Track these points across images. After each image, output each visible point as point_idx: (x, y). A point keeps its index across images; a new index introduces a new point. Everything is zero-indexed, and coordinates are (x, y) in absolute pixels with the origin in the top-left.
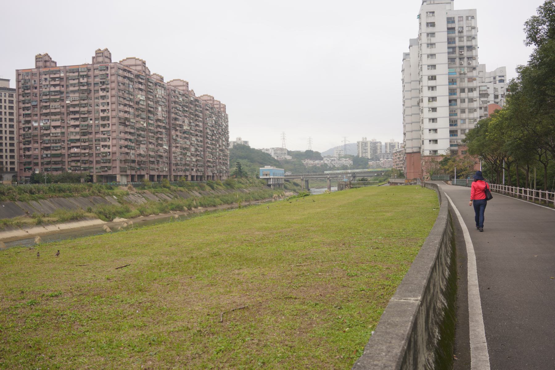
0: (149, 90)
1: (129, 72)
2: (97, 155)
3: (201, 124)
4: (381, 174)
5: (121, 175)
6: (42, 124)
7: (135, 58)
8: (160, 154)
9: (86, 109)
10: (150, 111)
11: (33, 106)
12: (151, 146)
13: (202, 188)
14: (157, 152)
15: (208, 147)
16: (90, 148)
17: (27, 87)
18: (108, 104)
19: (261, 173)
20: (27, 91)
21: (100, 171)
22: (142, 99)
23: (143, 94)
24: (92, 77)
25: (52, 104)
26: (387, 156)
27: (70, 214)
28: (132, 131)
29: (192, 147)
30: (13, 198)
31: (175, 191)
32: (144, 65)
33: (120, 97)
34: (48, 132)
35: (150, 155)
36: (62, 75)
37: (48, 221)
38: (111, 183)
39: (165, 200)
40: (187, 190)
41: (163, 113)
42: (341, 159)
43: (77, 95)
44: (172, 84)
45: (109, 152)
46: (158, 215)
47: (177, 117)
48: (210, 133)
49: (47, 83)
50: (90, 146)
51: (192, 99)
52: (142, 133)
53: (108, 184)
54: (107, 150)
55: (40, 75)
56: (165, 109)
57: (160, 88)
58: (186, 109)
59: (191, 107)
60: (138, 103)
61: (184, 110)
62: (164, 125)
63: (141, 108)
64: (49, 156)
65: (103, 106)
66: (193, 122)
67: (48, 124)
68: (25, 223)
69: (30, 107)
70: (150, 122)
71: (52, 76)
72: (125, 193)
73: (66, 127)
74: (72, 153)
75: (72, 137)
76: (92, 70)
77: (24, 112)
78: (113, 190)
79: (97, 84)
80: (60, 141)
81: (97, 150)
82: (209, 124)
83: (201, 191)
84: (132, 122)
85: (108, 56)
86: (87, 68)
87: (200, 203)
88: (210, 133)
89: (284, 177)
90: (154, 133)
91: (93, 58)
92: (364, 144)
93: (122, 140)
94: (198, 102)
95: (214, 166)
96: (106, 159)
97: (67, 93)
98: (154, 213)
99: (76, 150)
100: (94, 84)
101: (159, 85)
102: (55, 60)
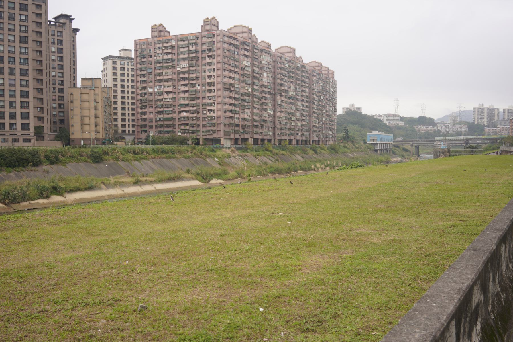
0: (254, 56)
1: (235, 39)
2: (204, 119)
3: (307, 90)
4: (497, 141)
5: (225, 138)
6: (156, 90)
7: (241, 26)
8: (264, 118)
9: (194, 75)
11: (148, 73)
12: (255, 111)
13: (305, 152)
14: (261, 117)
15: (314, 112)
16: (198, 113)
17: (143, 55)
19: (368, 138)
20: (143, 60)
21: (206, 134)
22: (247, 65)
25: (166, 71)
26: (505, 123)
27: (167, 175)
28: (237, 96)
29: (297, 112)
31: (277, 154)
32: (250, 32)
33: (225, 63)
34: (161, 97)
35: (254, 119)
36: (174, 43)
37: (146, 180)
38: (215, 146)
39: (266, 163)
40: (289, 154)
41: (269, 79)
42: (455, 125)
43: (187, 62)
44: (280, 51)
45: (214, 116)
47: (283, 83)
49: (161, 51)
50: (198, 110)
51: (299, 65)
52: (247, 98)
53: (212, 146)
54: (212, 114)
55: (155, 44)
56: (270, 75)
57: (266, 54)
58: (292, 75)
59: (297, 73)
60: (243, 69)
61: (291, 76)
62: (269, 90)
63: (246, 74)
64: (162, 119)
65: (210, 72)
66: (299, 88)
67: (162, 90)
68: (123, 182)
69: (146, 74)
70: (255, 87)
71: (165, 45)
72: (226, 155)
73: (177, 93)
75: (182, 102)
76: (200, 38)
77: (141, 79)
78: (215, 152)
79: (205, 51)
80: (171, 106)
81: (204, 114)
82: (315, 90)
83: (304, 155)
84: (237, 88)
85: (216, 24)
86: (196, 36)
87: (300, 166)
89: (392, 143)
90: (259, 98)
91: (202, 26)
92: (480, 110)
93: (226, 105)
96: (212, 123)
97: (178, 60)
99: (185, 114)
100: (202, 51)
101: (265, 51)
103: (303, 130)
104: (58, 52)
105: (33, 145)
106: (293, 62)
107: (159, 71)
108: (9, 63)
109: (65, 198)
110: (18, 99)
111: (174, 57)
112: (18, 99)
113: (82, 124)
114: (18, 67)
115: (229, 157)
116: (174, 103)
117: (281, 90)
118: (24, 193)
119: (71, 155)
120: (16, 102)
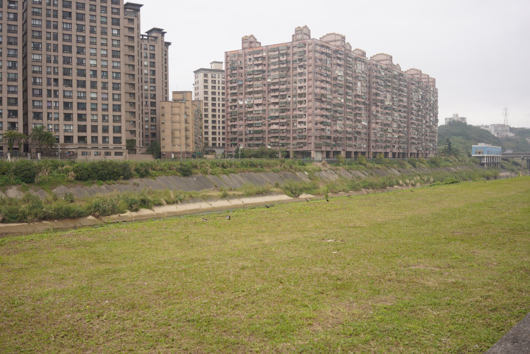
0: (348, 65)
1: (327, 47)
2: (294, 132)
3: (405, 99)
5: (316, 151)
6: (246, 102)
7: (334, 34)
8: (358, 130)
9: (285, 86)
10: (348, 87)
11: (239, 85)
12: (348, 122)
13: (402, 165)
14: (355, 129)
15: (413, 123)
16: (288, 125)
17: (233, 67)
18: (305, 80)
20: (234, 72)
21: (296, 147)
22: (340, 74)
24: (291, 55)
25: (256, 83)
27: (255, 189)
28: (329, 107)
29: (394, 123)
30: (205, 172)
31: (371, 168)
32: (343, 40)
33: (317, 73)
34: (251, 110)
35: (347, 131)
36: (264, 54)
37: (234, 194)
38: (305, 159)
39: (359, 178)
40: (385, 167)
41: (363, 88)
43: (277, 73)
44: (375, 59)
45: (305, 129)
46: (348, 192)
47: (378, 92)
49: (251, 63)
50: (288, 122)
51: (396, 73)
52: (340, 109)
53: (302, 160)
54: (303, 126)
55: (245, 55)
56: (365, 85)
57: (360, 63)
58: (388, 84)
59: (394, 82)
60: (335, 79)
62: (363, 100)
63: (338, 84)
64: (252, 132)
65: (301, 83)
66: (396, 97)
67: (252, 102)
68: (210, 196)
69: (236, 86)
70: (348, 97)
71: (256, 56)
72: (317, 169)
73: (267, 105)
74: (271, 130)
75: (272, 114)
76: (291, 48)
77: (231, 92)
79: (296, 61)
80: (261, 118)
81: (294, 126)
82: (414, 99)
83: (401, 169)
84: (329, 98)
85: (308, 33)
89: (501, 156)
90: (352, 109)
91: (293, 36)
93: (318, 116)
94: (403, 76)
95: (419, 143)
96: (302, 136)
97: (269, 71)
98: (344, 191)
99: (275, 127)
100: (293, 61)
101: (359, 59)
103: (401, 142)
105: (125, 158)
107: (249, 83)
108: (102, 78)
109: (154, 211)
110: (111, 113)
111: (265, 68)
112: (111, 113)
113: (173, 138)
114: (110, 81)
115: (320, 170)
116: (264, 115)
118: (114, 206)
120: (109, 116)
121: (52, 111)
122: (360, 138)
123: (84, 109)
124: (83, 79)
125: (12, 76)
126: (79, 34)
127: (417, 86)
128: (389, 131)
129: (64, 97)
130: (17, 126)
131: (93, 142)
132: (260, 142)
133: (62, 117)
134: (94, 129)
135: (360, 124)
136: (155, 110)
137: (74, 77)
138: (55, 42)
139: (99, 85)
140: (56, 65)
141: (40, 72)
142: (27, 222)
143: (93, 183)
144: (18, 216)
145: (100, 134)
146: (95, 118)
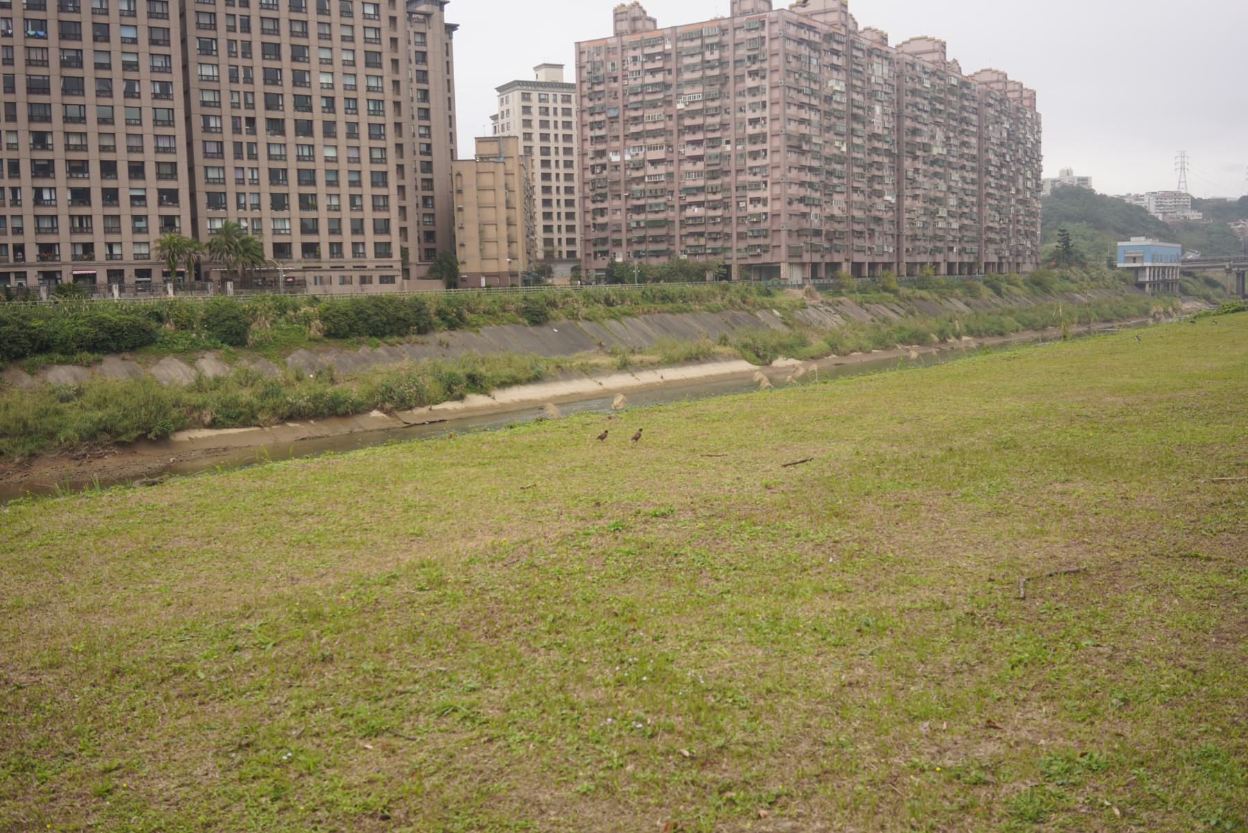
0: (854, 67)
1: (811, 28)
2: (740, 221)
3: (973, 141)
5: (791, 264)
6: (628, 158)
9: (717, 119)
11: (610, 118)
12: (855, 197)
13: (971, 291)
15: (989, 195)
16: (726, 206)
17: (597, 78)
18: (764, 104)
19: (1120, 255)
20: (597, 88)
21: (745, 254)
22: (838, 88)
23: (840, 78)
24: (731, 47)
25: (649, 112)
27: (683, 348)
28: (815, 164)
29: (951, 195)
30: (573, 314)
31: (909, 299)
32: (843, 9)
33: (789, 88)
34: (640, 173)
35: (853, 217)
36: (668, 46)
37: (641, 362)
38: (769, 283)
39: (886, 320)
40: (936, 296)
41: (886, 118)
44: (908, 49)
45: (766, 214)
46: (870, 352)
47: (918, 126)
48: (995, 160)
49: (638, 67)
50: (726, 200)
51: (954, 82)
52: (838, 167)
53: (763, 283)
54: (760, 208)
55: (623, 50)
56: (890, 110)
57: (879, 60)
58: (938, 106)
59: (950, 102)
60: (828, 99)
61: (935, 110)
62: (886, 147)
64: (642, 224)
65: (754, 111)
67: (641, 157)
68: (596, 365)
69: (604, 121)
70: (856, 141)
71: (648, 51)
72: (798, 304)
73: (676, 162)
75: (689, 183)
76: (731, 31)
77: (592, 134)
79: (741, 61)
82: (993, 140)
84: (816, 144)
86: (720, 27)
87: (967, 326)
88: (995, 160)
89: (1180, 265)
90: (863, 167)
93: (793, 186)
94: (968, 88)
95: (1002, 240)
96: (759, 230)
97: (679, 86)
98: (861, 349)
99: (696, 211)
100: (735, 62)
101: (878, 53)
102: (653, 16)
103: (965, 239)
104: (418, 81)
105: (402, 290)
106: (941, 74)
107: (633, 114)
108: (346, 113)
110: (367, 190)
111: (670, 78)
112: (367, 190)
113: (483, 241)
114: (364, 119)
115: (804, 307)
116: (670, 185)
117: (914, 145)
118: (419, 392)
119: (487, 308)
120: (364, 196)
121: (247, 188)
122: (880, 233)
123: (313, 182)
124: (306, 116)
125: (163, 115)
126: (295, 16)
127: (999, 109)
128: (940, 214)
129: (270, 157)
130: (177, 225)
131: (332, 254)
132: (663, 247)
133: (266, 201)
134: (335, 229)
135: (880, 200)
136: (431, 181)
137: (289, 114)
138: (246, 37)
139: (341, 129)
140: (249, 88)
141: (218, 104)
142: (258, 426)
143: (359, 343)
144: (241, 413)
145: (347, 238)
146: (335, 202)
